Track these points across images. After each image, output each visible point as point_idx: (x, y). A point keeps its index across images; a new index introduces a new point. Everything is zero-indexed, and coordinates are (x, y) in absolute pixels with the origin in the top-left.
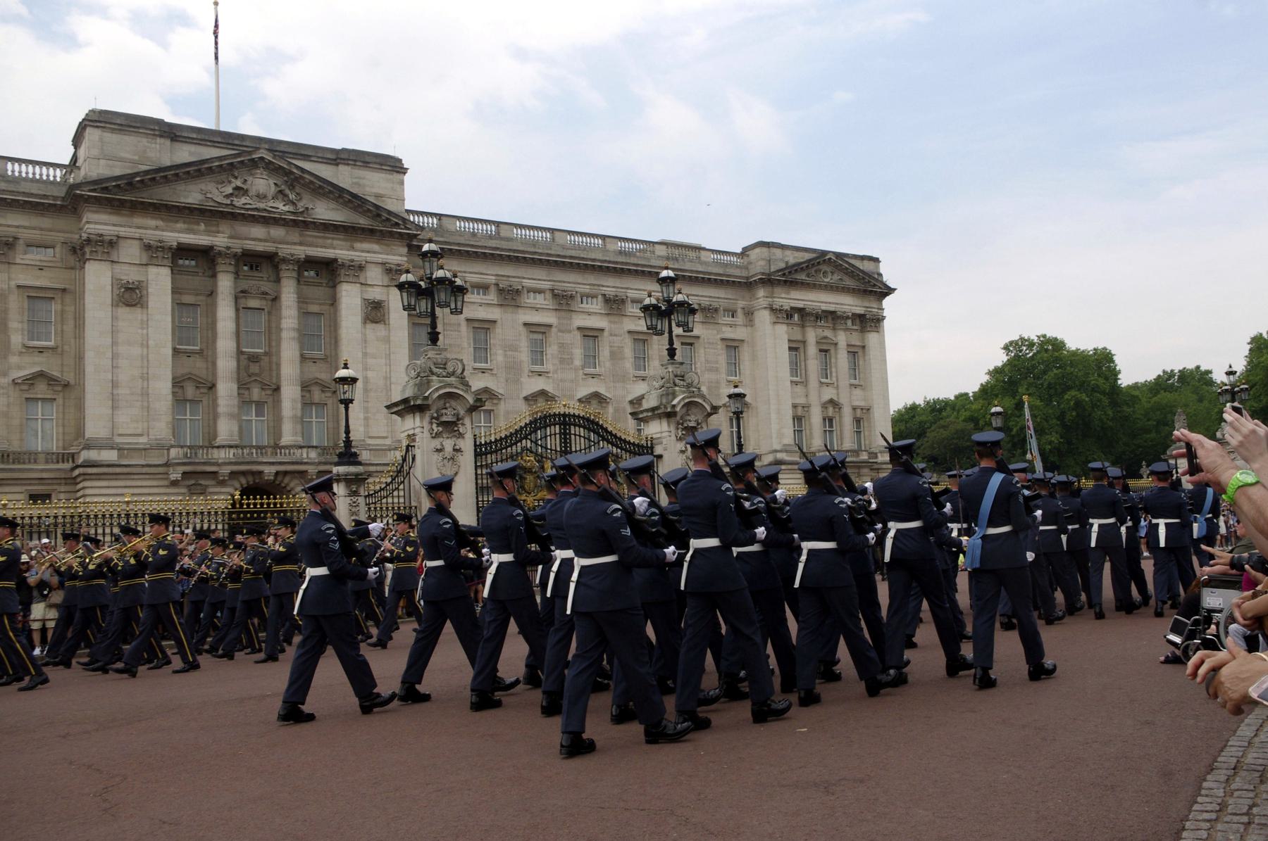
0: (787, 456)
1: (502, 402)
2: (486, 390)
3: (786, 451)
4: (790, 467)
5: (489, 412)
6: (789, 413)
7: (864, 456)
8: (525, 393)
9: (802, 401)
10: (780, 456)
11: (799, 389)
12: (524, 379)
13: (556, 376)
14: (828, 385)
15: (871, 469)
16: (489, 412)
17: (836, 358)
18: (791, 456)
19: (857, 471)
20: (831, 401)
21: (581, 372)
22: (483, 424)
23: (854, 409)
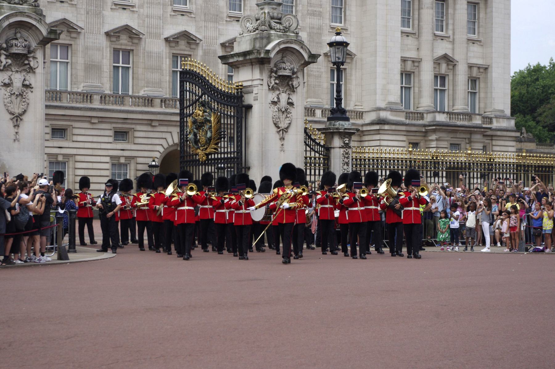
0: (392, 115)
1: (82, 37)
2: (64, 22)
3: (391, 110)
4: (393, 127)
5: (66, 47)
6: (397, 68)
7: (477, 121)
8: (108, 28)
9: (412, 54)
10: (384, 115)
11: (410, 41)
12: (107, 13)
13: (142, 10)
14: (442, 38)
15: (484, 136)
16: (66, 47)
17: (455, 9)
18: (396, 116)
19: (468, 136)
20: (445, 57)
21: (169, 9)
22: (59, 60)
23: (471, 67)
